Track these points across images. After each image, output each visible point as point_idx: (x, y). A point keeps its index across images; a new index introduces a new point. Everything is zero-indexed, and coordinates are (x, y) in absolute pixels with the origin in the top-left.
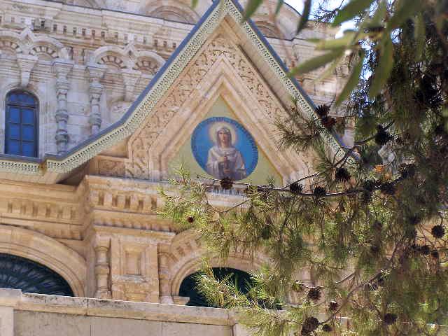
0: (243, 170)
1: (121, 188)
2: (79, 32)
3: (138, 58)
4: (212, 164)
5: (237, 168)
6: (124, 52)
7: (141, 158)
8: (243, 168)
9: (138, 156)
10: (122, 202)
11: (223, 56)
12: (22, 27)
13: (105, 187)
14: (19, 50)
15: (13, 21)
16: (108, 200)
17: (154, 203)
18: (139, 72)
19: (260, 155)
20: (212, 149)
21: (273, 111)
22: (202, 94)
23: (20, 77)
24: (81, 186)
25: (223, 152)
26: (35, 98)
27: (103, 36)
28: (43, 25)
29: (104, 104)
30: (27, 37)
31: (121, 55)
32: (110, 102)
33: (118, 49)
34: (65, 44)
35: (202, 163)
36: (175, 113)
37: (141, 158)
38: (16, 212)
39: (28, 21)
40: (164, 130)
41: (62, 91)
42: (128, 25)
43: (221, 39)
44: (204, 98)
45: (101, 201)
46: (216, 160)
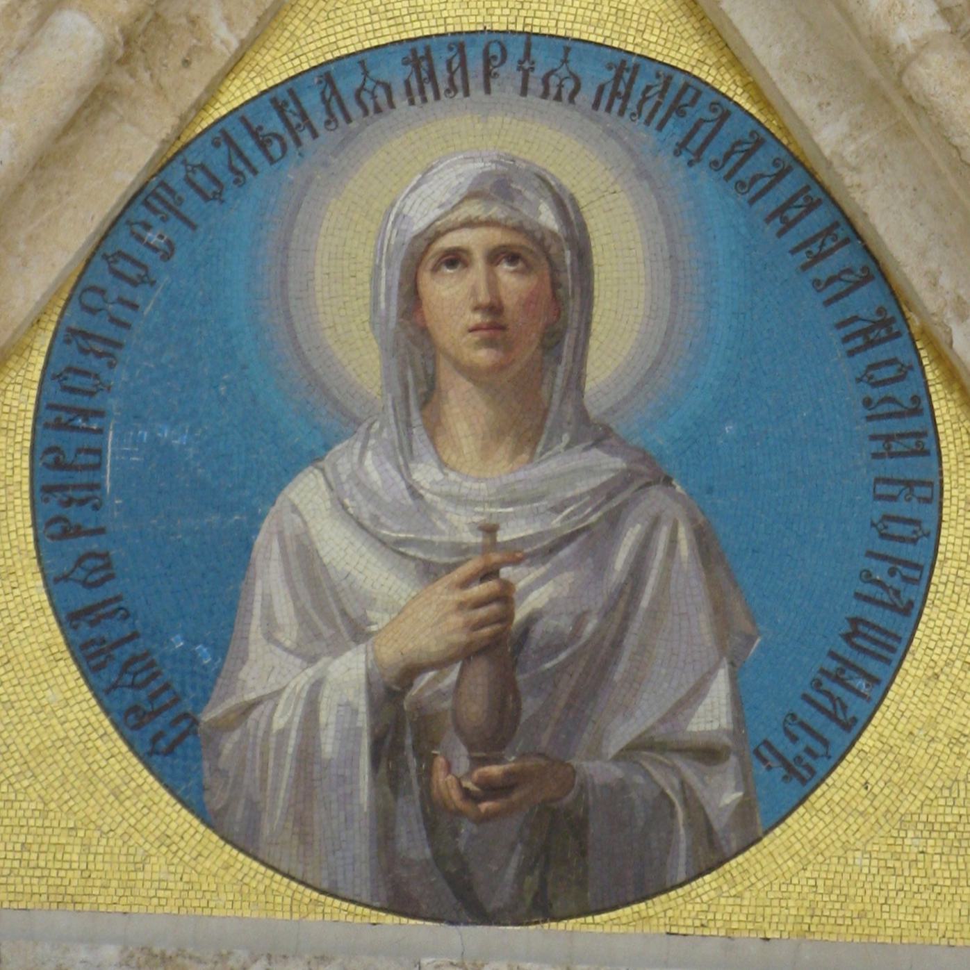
0: (708, 754)
4: (296, 684)
5: (622, 733)
8: (712, 716)
20: (307, 493)
25: (460, 527)
46: (359, 632)
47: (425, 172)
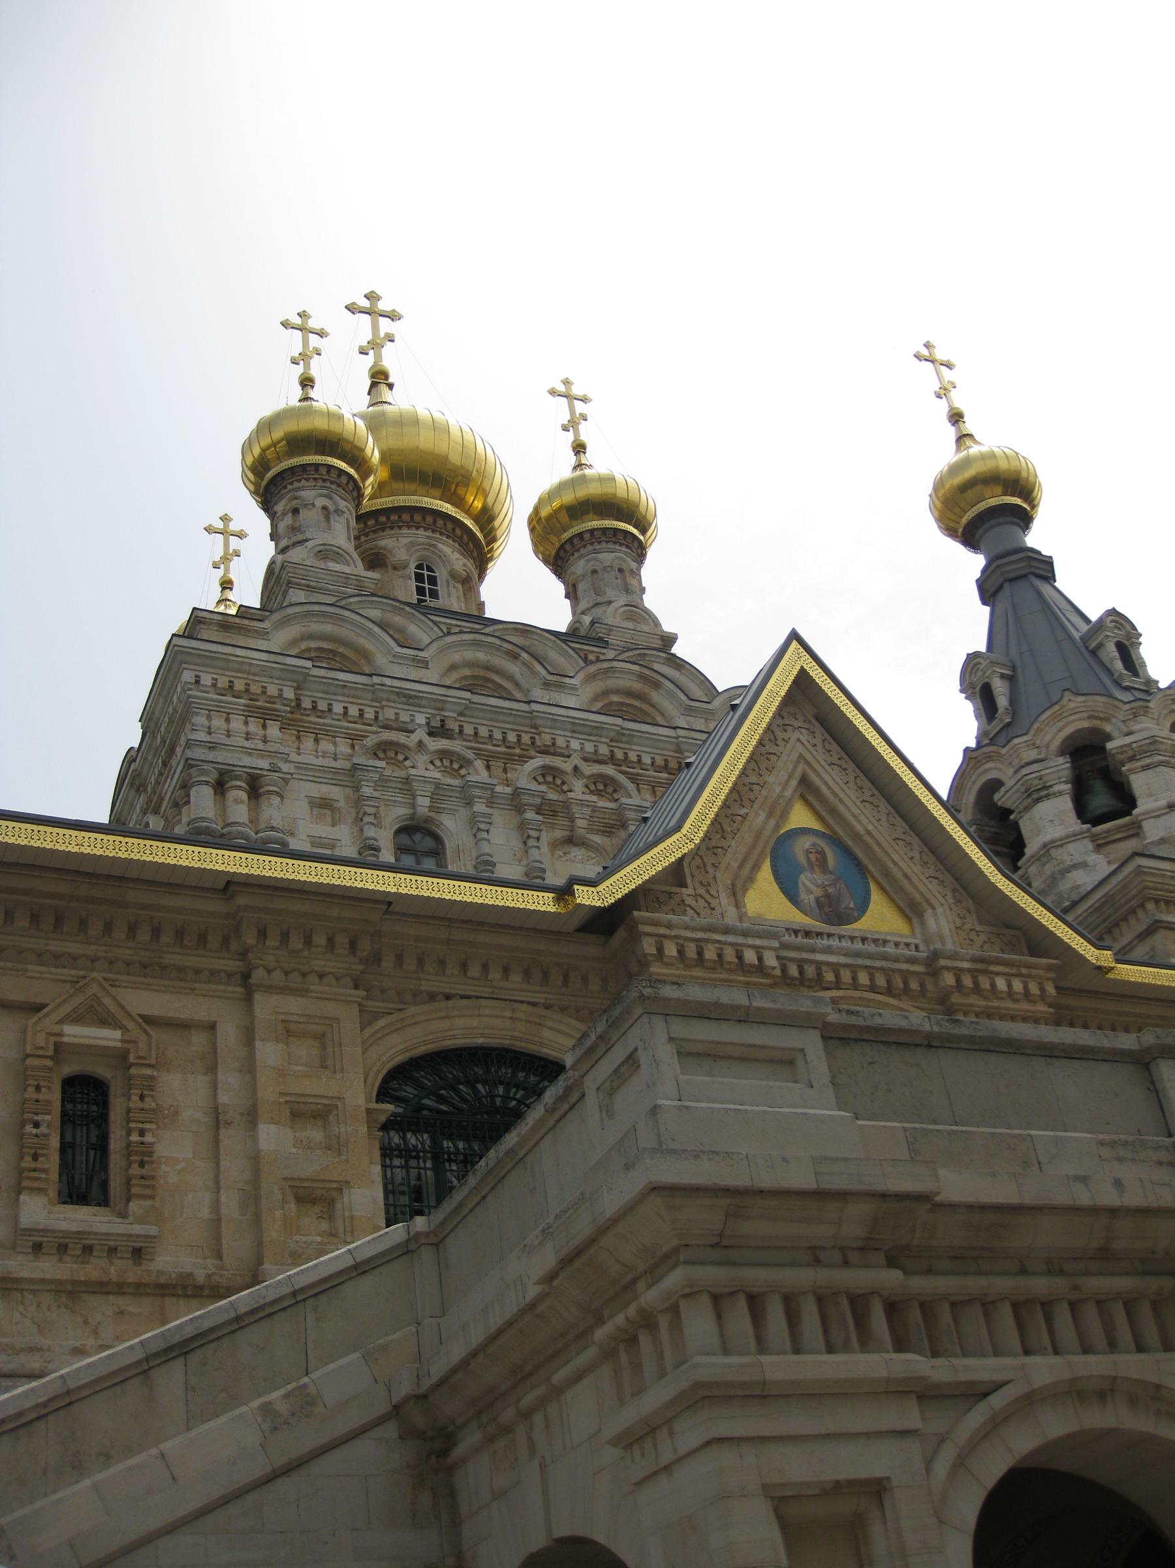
1: (689, 934)
2: (498, 735)
3: (589, 777)
6: (567, 766)
7: (706, 885)
8: (852, 905)
9: (701, 882)
10: (691, 952)
11: (797, 735)
12: (411, 727)
13: (662, 931)
14: (408, 763)
15: (397, 719)
16: (671, 950)
17: (740, 957)
18: (594, 798)
19: (873, 887)
20: (802, 876)
21: (884, 818)
22: (778, 790)
23: (413, 806)
24: (621, 933)
25: (820, 882)
26: (438, 839)
27: (533, 743)
28: (442, 726)
29: (545, 849)
30: (420, 744)
31: (562, 772)
32: (554, 845)
33: (558, 762)
34: (479, 754)
35: (793, 899)
36: (744, 817)
37: (706, 885)
38: (516, 978)
39: (421, 719)
40: (733, 844)
41: (482, 826)
42: (570, 726)
43: (791, 709)
44: (780, 796)
45: (660, 949)
47: (805, 843)
